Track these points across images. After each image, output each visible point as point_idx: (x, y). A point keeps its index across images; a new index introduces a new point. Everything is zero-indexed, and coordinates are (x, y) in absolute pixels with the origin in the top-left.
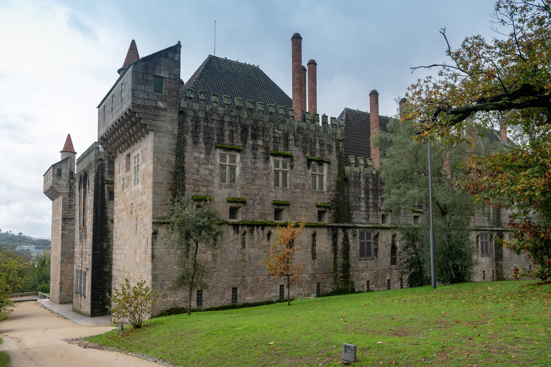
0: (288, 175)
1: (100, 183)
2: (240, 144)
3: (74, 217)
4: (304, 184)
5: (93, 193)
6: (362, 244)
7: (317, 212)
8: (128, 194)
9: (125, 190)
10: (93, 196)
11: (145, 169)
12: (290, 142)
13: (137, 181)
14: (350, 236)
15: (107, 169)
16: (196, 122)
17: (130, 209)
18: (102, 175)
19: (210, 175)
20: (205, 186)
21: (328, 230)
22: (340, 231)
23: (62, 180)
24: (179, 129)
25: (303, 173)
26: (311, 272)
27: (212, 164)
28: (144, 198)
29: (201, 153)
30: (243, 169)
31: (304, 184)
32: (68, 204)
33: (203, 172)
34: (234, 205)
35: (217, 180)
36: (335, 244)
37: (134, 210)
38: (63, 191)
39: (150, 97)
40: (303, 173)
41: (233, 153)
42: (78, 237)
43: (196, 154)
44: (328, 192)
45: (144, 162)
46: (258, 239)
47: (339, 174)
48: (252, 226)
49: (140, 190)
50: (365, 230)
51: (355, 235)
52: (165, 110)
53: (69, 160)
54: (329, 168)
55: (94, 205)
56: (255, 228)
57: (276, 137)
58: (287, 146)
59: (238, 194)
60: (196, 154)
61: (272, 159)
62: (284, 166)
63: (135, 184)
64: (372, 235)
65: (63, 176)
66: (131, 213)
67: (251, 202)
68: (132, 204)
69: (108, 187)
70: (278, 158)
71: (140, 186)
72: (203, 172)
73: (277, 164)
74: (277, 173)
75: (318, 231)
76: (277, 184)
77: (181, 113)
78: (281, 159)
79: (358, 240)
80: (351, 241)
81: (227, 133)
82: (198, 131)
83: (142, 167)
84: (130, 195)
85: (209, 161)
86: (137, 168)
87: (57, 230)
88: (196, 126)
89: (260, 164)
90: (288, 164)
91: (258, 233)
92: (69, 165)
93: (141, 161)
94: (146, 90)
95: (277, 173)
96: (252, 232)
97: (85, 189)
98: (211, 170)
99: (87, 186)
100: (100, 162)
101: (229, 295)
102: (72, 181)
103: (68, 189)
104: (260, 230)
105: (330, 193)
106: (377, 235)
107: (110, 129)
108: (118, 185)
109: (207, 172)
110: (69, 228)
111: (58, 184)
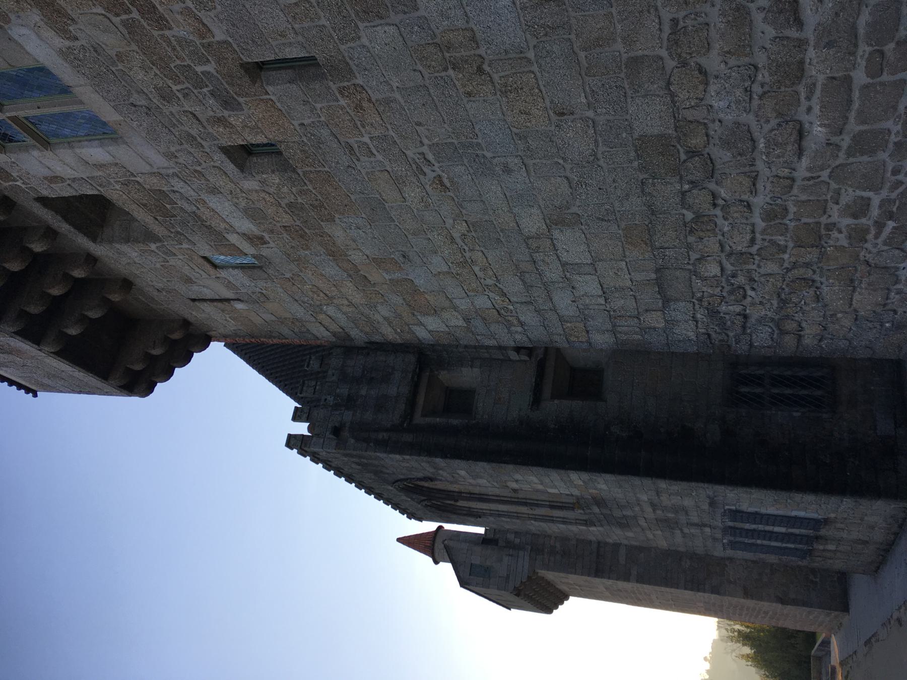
1: (408, 438)
10: (456, 463)
18: (387, 430)
55: (477, 459)
65: (488, 563)
69: (424, 415)
100: (346, 434)
102: (501, 543)
103: (521, 553)
111: (508, 576)
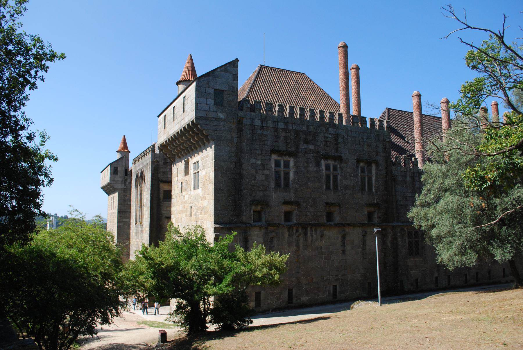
0: (339, 177)
2: (293, 149)
3: (128, 210)
4: (354, 185)
5: (150, 192)
6: (410, 243)
7: (366, 213)
8: (187, 197)
9: (184, 193)
11: (206, 176)
12: (339, 146)
13: (196, 186)
15: (162, 170)
16: (253, 130)
17: (189, 212)
19: (266, 179)
20: (261, 191)
22: (390, 230)
23: (118, 176)
24: (238, 137)
25: (352, 175)
27: (267, 169)
28: (205, 203)
29: (258, 159)
30: (296, 173)
31: (354, 185)
32: (123, 198)
33: (260, 177)
34: (288, 208)
35: (273, 185)
37: (193, 213)
38: (119, 187)
39: (211, 109)
40: (352, 175)
41: (287, 158)
42: (134, 231)
43: (253, 161)
44: (377, 192)
45: (204, 168)
46: (312, 241)
47: (387, 173)
48: (305, 227)
49: (201, 195)
52: (224, 120)
53: (124, 159)
56: (309, 229)
57: (327, 141)
58: (337, 149)
59: (292, 197)
60: (253, 161)
61: (323, 162)
62: (335, 169)
63: (194, 188)
65: (119, 173)
66: (191, 215)
67: (304, 205)
68: (191, 207)
70: (329, 162)
71: (200, 191)
72: (260, 177)
73: (327, 167)
74: (328, 177)
76: (328, 188)
77: (240, 122)
78: (331, 163)
79: (407, 238)
81: (282, 138)
82: (254, 138)
83: (202, 173)
84: (189, 198)
85: (264, 167)
86: (197, 174)
87: (113, 222)
88: (253, 134)
89: (312, 168)
90: (339, 166)
91: (312, 236)
92: (124, 164)
93: (201, 167)
94: (208, 103)
95: (328, 177)
96: (306, 234)
97: (141, 187)
98: (267, 176)
99: (143, 184)
101: (285, 296)
103: (123, 185)
104: (314, 232)
105: (378, 193)
107: (171, 137)
108: (176, 188)
109: (263, 178)
110: (124, 220)
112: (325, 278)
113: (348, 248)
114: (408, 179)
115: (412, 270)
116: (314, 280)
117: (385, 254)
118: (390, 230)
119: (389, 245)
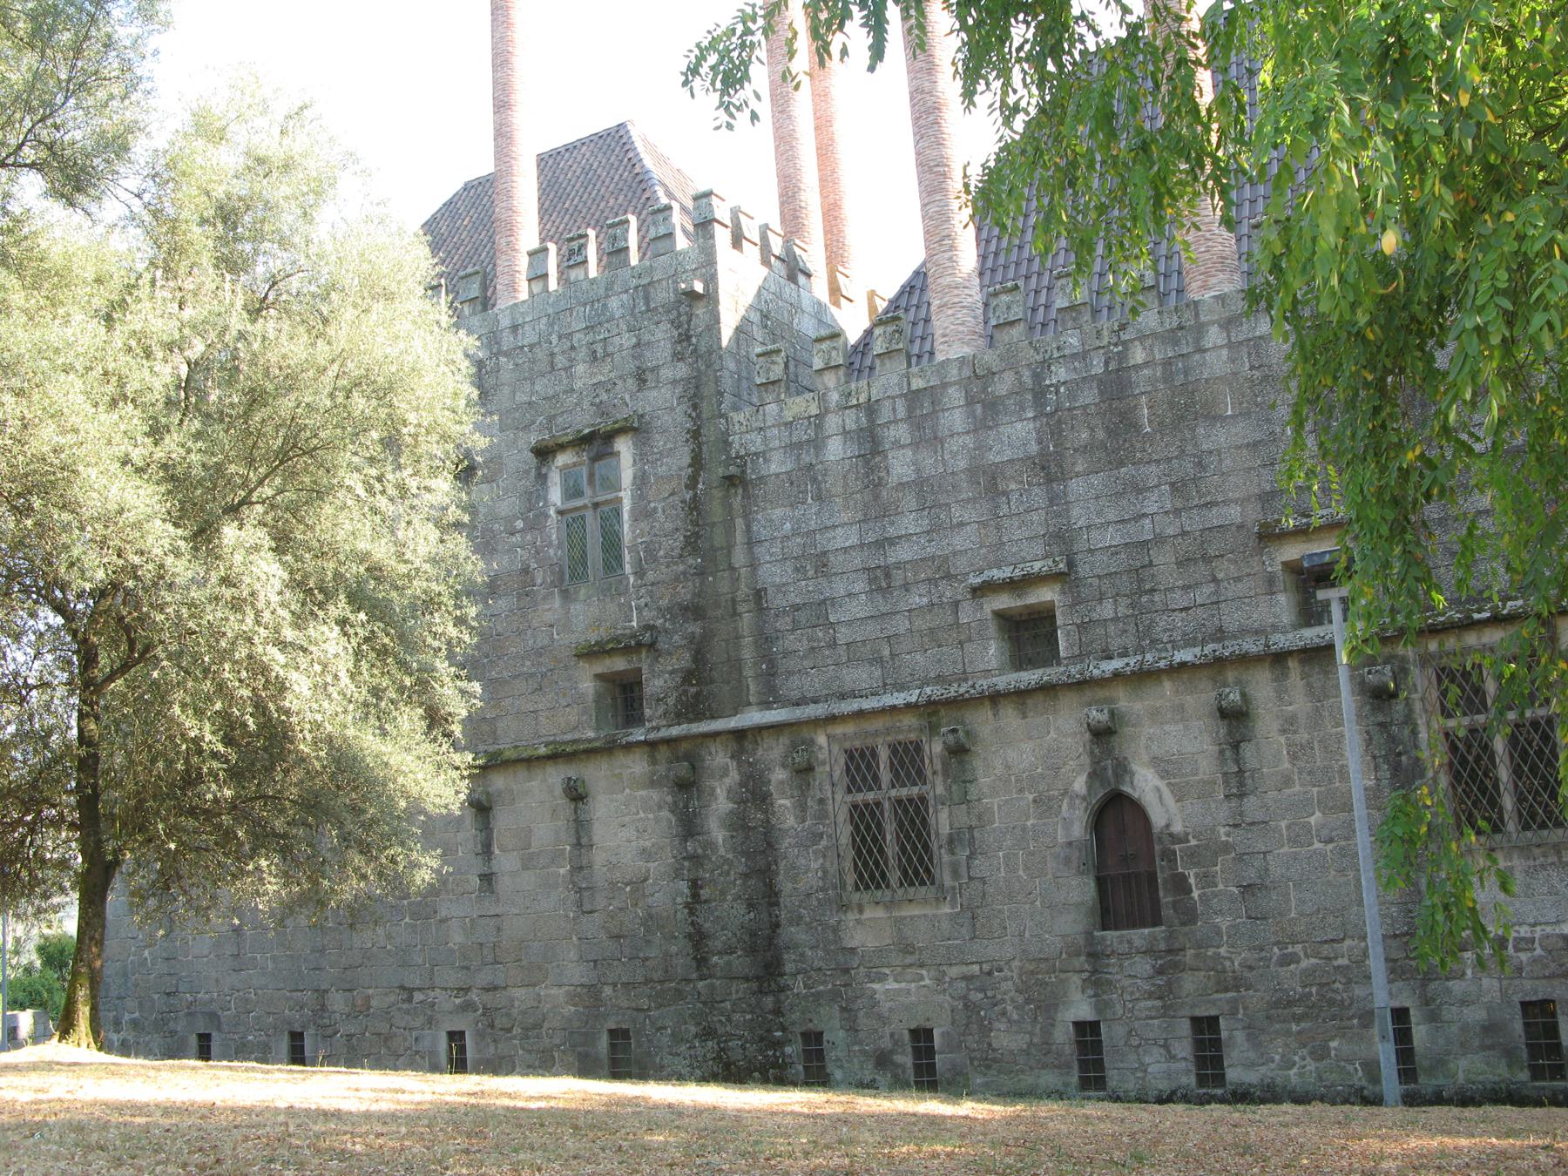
4: (526, 571)
14: (779, 775)
21: (654, 762)
22: (718, 757)
26: (577, 973)
31: (526, 571)
36: (689, 826)
50: (878, 724)
51: (804, 771)
54: (641, 457)
64: (935, 748)
75: (596, 774)
80: (783, 803)
106: (959, 751)
112: (418, 997)
113: (505, 862)
114: (835, 449)
115: (882, 978)
116: (374, 1003)
117: (695, 885)
118: (718, 757)
119: (719, 835)
